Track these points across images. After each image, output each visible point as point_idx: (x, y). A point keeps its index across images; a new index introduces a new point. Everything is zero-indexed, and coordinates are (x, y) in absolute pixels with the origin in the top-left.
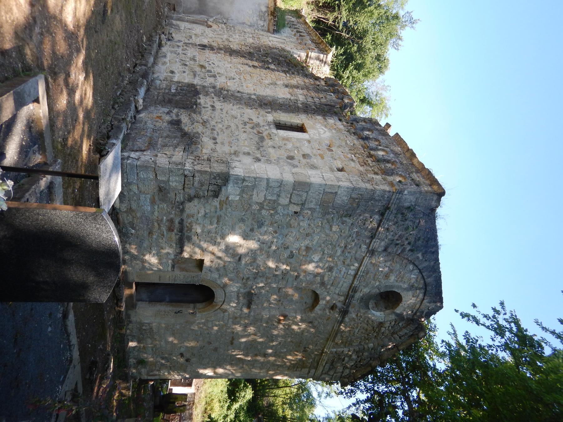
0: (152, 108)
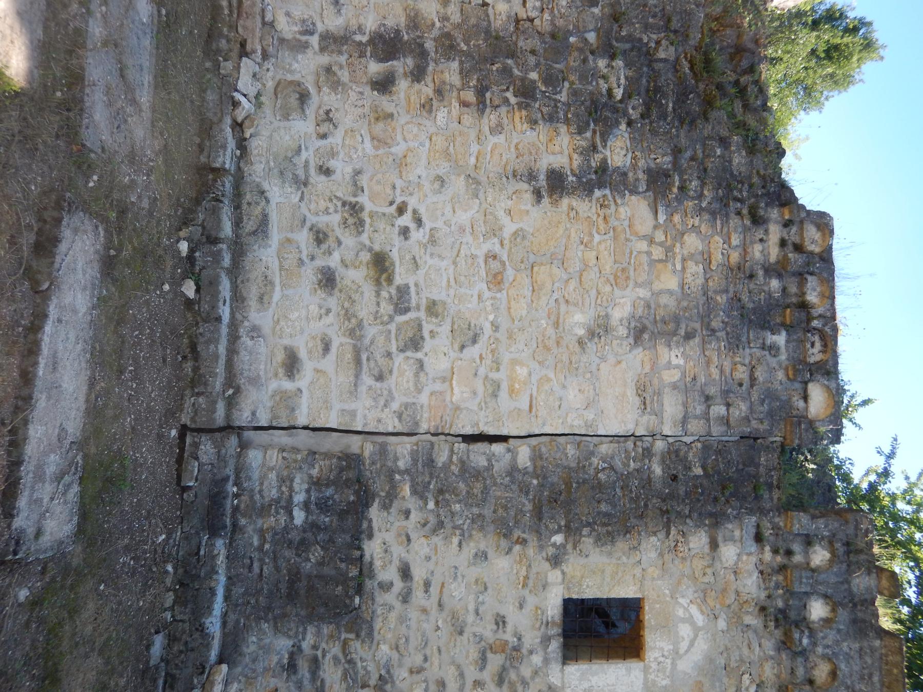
0: (251, 645)
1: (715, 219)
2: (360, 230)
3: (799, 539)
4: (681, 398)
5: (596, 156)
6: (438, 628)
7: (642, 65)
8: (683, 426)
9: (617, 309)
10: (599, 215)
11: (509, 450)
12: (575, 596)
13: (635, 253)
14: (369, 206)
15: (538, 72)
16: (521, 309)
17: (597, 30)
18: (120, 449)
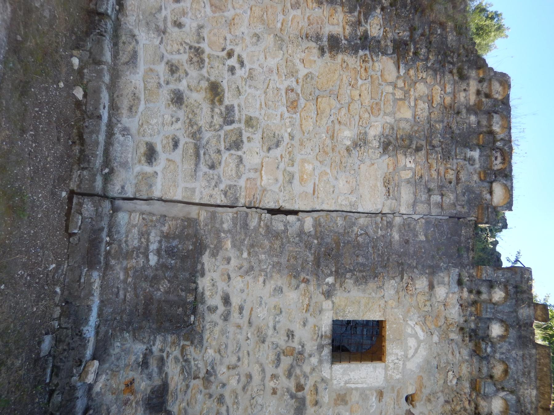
0: (116, 348)
1: (436, 74)
2: (201, 66)
3: (485, 284)
4: (412, 190)
5: (361, 28)
6: (248, 338)
8: (413, 208)
9: (372, 129)
10: (361, 67)
11: (299, 220)
12: (340, 319)
13: (384, 93)
14: (208, 50)
16: (309, 125)
18: (20, 188)
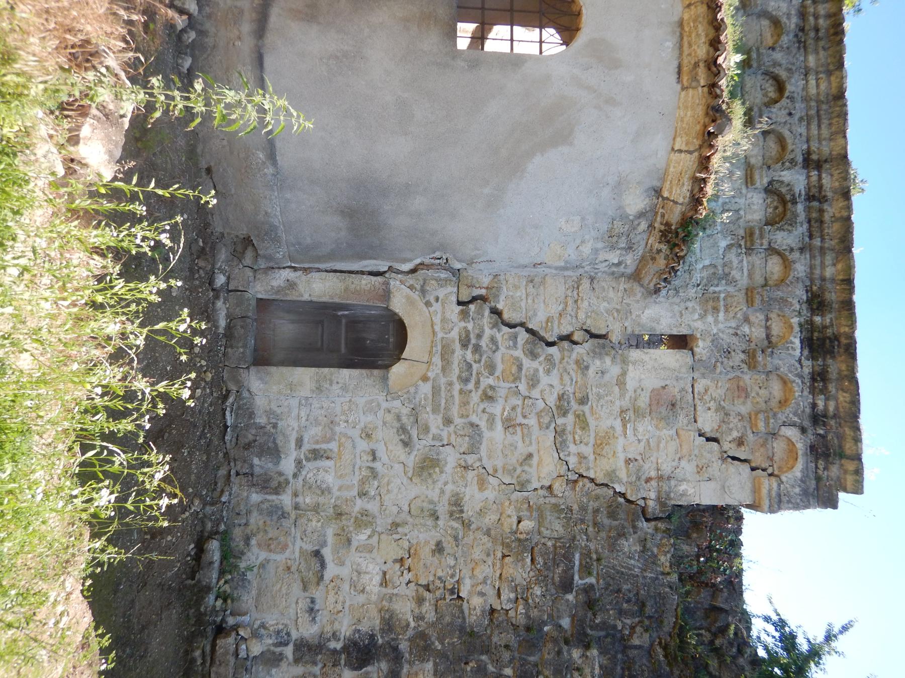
7: (616, 652)
15: (513, 668)
17: (573, 617)
